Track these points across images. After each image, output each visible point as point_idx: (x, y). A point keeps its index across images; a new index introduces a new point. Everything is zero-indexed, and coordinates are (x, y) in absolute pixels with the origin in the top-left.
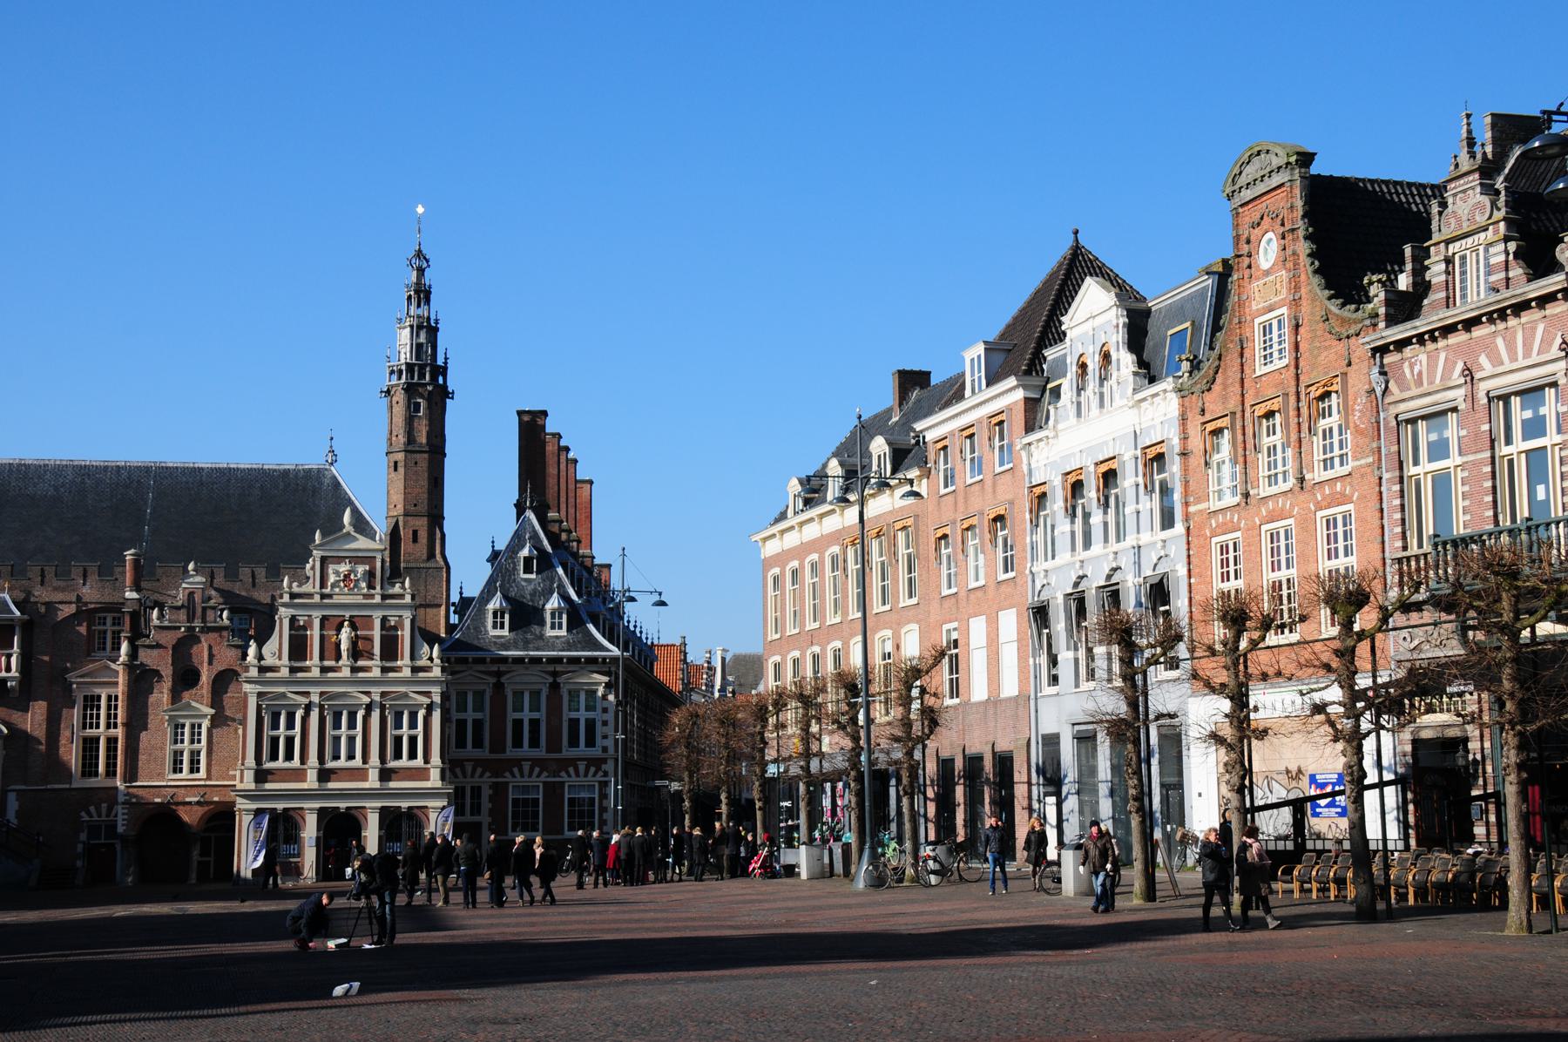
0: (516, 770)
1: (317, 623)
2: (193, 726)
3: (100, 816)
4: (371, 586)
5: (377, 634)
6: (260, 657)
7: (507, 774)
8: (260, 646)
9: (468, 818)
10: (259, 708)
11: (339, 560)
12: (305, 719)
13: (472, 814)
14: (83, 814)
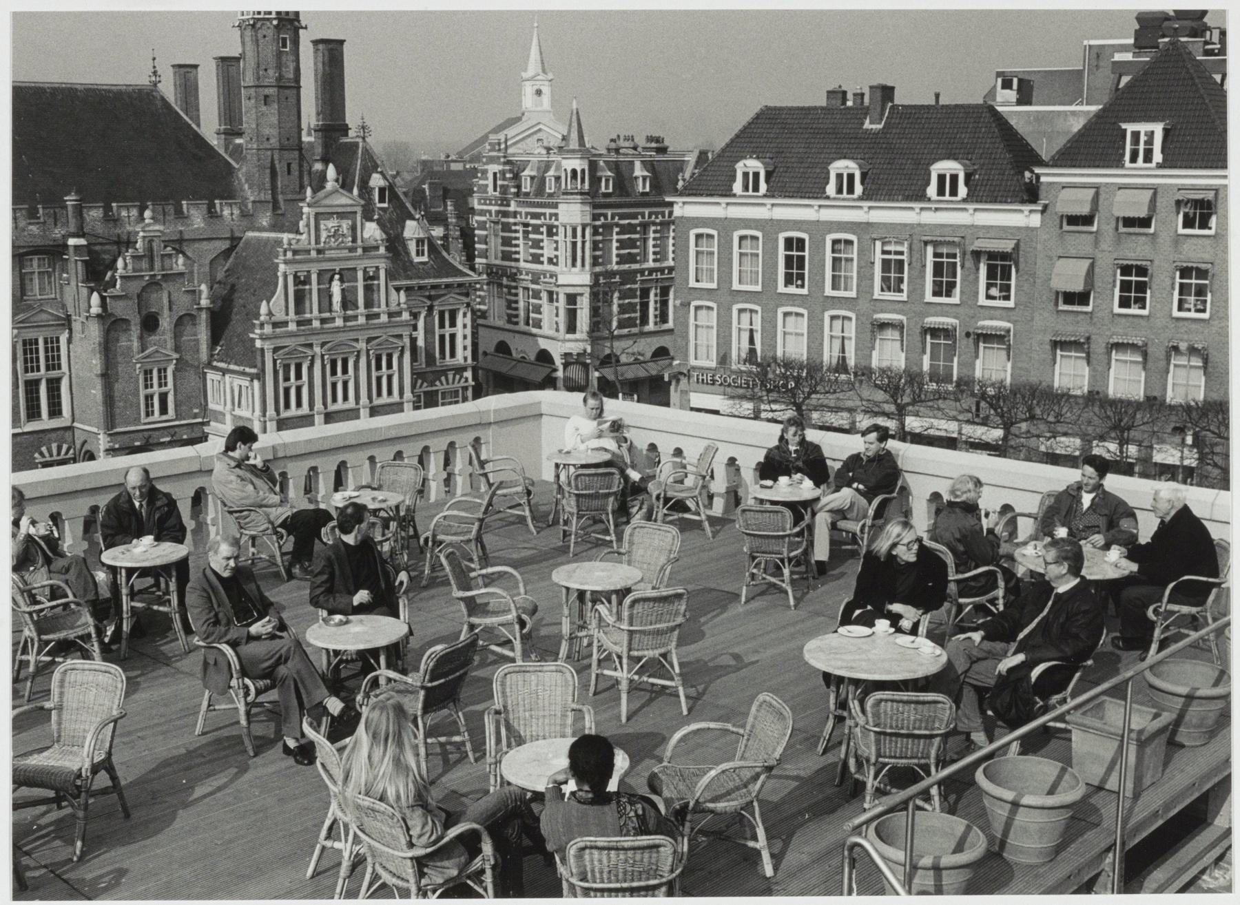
1: (314, 277)
2: (159, 371)
3: (51, 455)
4: (354, 240)
5: (360, 284)
6: (270, 314)
8: (268, 302)
10: (275, 361)
11: (329, 215)
12: (311, 368)
14: (36, 455)
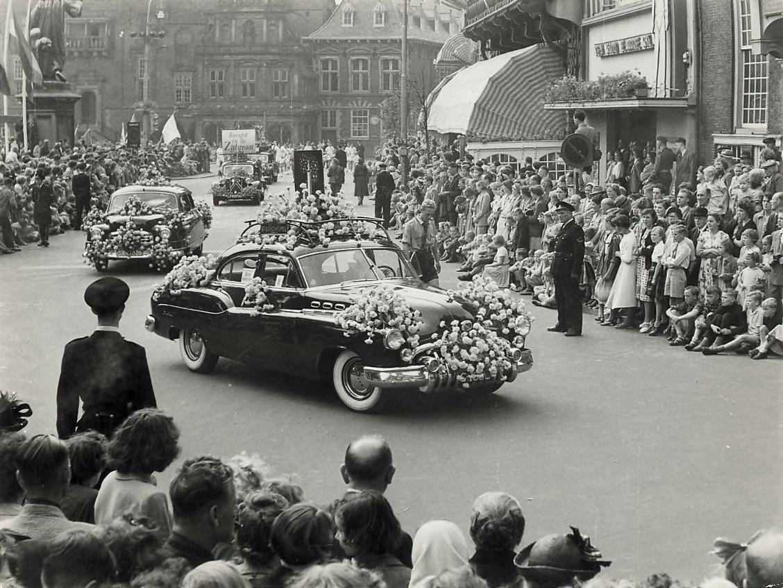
0: (354, 102)
7: (350, 104)
9: (329, 127)
13: (331, 126)
